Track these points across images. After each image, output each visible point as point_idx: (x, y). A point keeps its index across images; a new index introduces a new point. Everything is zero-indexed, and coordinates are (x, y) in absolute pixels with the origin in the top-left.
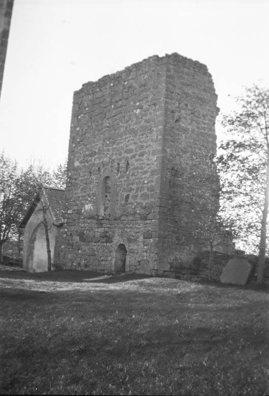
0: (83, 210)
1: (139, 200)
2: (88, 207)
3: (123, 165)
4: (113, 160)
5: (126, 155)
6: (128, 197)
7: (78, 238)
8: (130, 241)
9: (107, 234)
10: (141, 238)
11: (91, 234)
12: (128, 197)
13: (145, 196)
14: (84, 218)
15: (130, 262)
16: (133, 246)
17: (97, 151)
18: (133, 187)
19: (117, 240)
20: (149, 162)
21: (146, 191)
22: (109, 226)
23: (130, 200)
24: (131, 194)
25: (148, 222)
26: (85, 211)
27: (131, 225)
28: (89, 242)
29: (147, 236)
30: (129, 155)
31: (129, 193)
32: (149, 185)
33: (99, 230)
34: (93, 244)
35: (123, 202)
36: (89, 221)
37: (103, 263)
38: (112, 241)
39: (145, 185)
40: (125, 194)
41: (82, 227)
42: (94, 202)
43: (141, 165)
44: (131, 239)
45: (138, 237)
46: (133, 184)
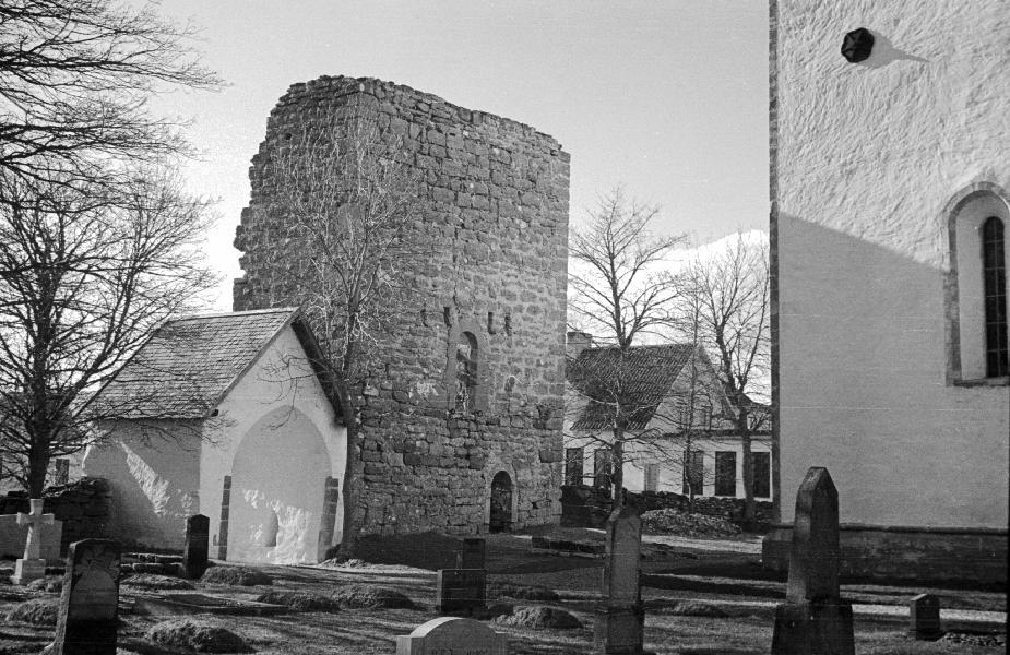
0: (411, 395)
1: (533, 394)
5: (503, 300)
7: (400, 457)
11: (435, 449)
19: (494, 464)
21: (540, 378)
23: (515, 389)
26: (417, 396)
27: (519, 436)
30: (512, 305)
34: (440, 470)
35: (502, 391)
37: (464, 510)
42: (437, 379)
45: (533, 460)
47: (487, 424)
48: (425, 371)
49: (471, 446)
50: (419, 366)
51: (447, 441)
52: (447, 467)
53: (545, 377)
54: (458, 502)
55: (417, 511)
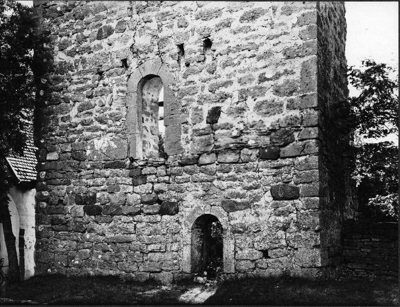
0: (88, 152)
2: (102, 143)
3: (193, 45)
4: (164, 40)
6: (215, 113)
7: (80, 209)
8: (231, 207)
9: (161, 196)
10: (268, 197)
11: (116, 198)
12: (215, 113)
13: (272, 108)
14: (93, 167)
15: (236, 252)
16: (239, 217)
17: (113, 25)
18: (227, 90)
19: (193, 204)
20: (275, 32)
22: (167, 178)
23: (223, 119)
24: (225, 106)
25: (284, 162)
26: (94, 152)
28: (112, 215)
29: (283, 193)
30: (212, 23)
31: (218, 105)
32: (281, 81)
33: (137, 189)
34: (124, 218)
35: (204, 125)
36: (108, 172)
38: (177, 211)
39: (266, 84)
40: (207, 108)
41: (88, 186)
42: (116, 132)
43: (251, 41)
44: (235, 202)
45: (257, 198)
46: (227, 84)
47: (181, 165)
48: (103, 127)
49: (162, 192)
50: (97, 124)
51: (130, 189)
52: (130, 214)
53: (277, 92)
54: (150, 248)
55: (100, 256)
